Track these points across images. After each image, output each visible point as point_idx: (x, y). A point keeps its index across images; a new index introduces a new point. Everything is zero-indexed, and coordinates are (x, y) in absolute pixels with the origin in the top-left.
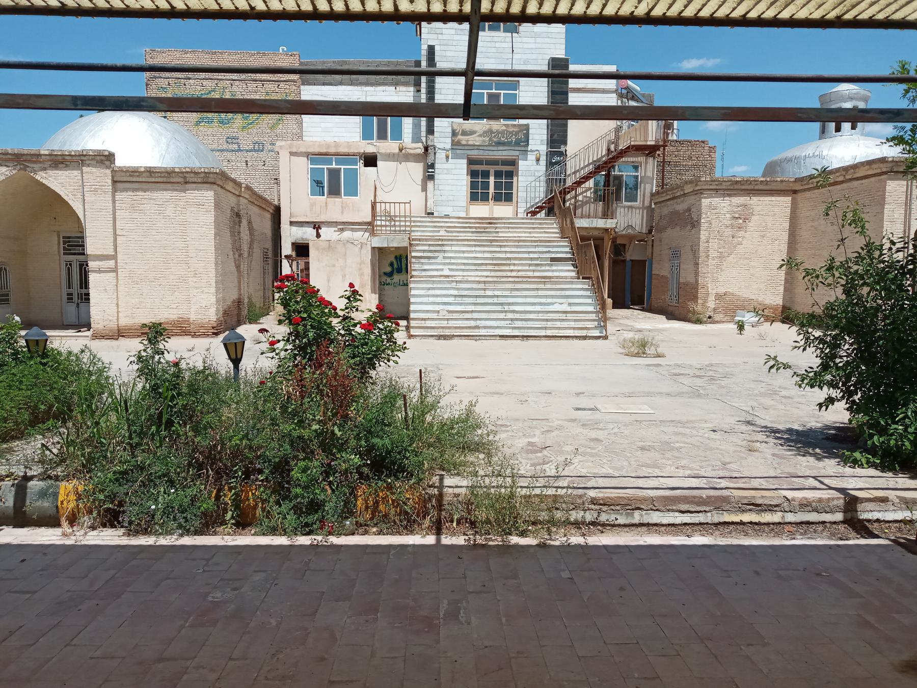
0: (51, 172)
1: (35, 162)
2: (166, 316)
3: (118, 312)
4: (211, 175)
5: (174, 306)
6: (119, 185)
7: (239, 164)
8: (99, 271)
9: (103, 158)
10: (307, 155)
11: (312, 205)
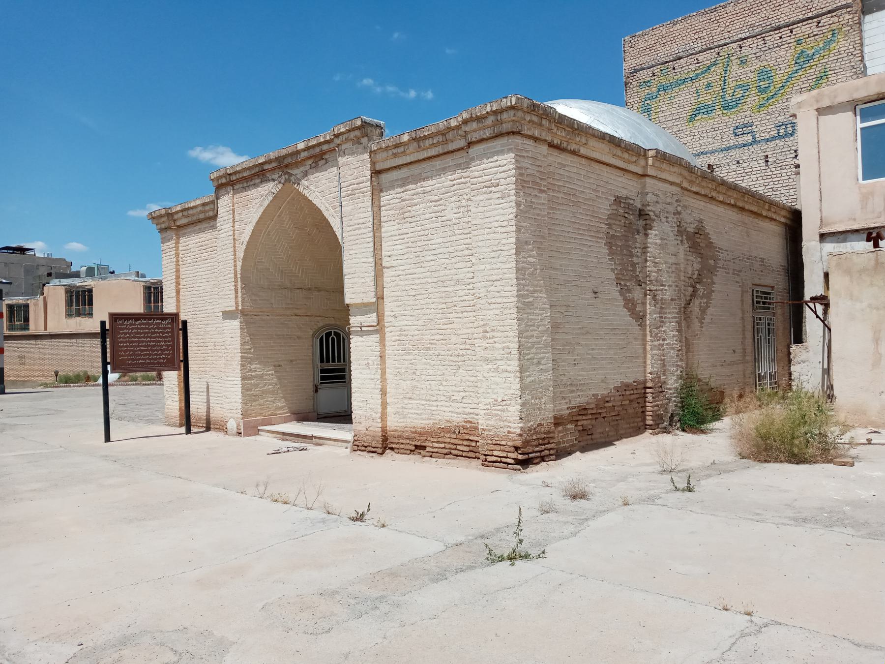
0: (311, 177)
1: (297, 164)
2: (448, 416)
3: (384, 405)
4: (505, 116)
5: (458, 397)
6: (384, 177)
7: (754, 164)
9: (357, 133)
10: (853, 106)
11: (866, 198)
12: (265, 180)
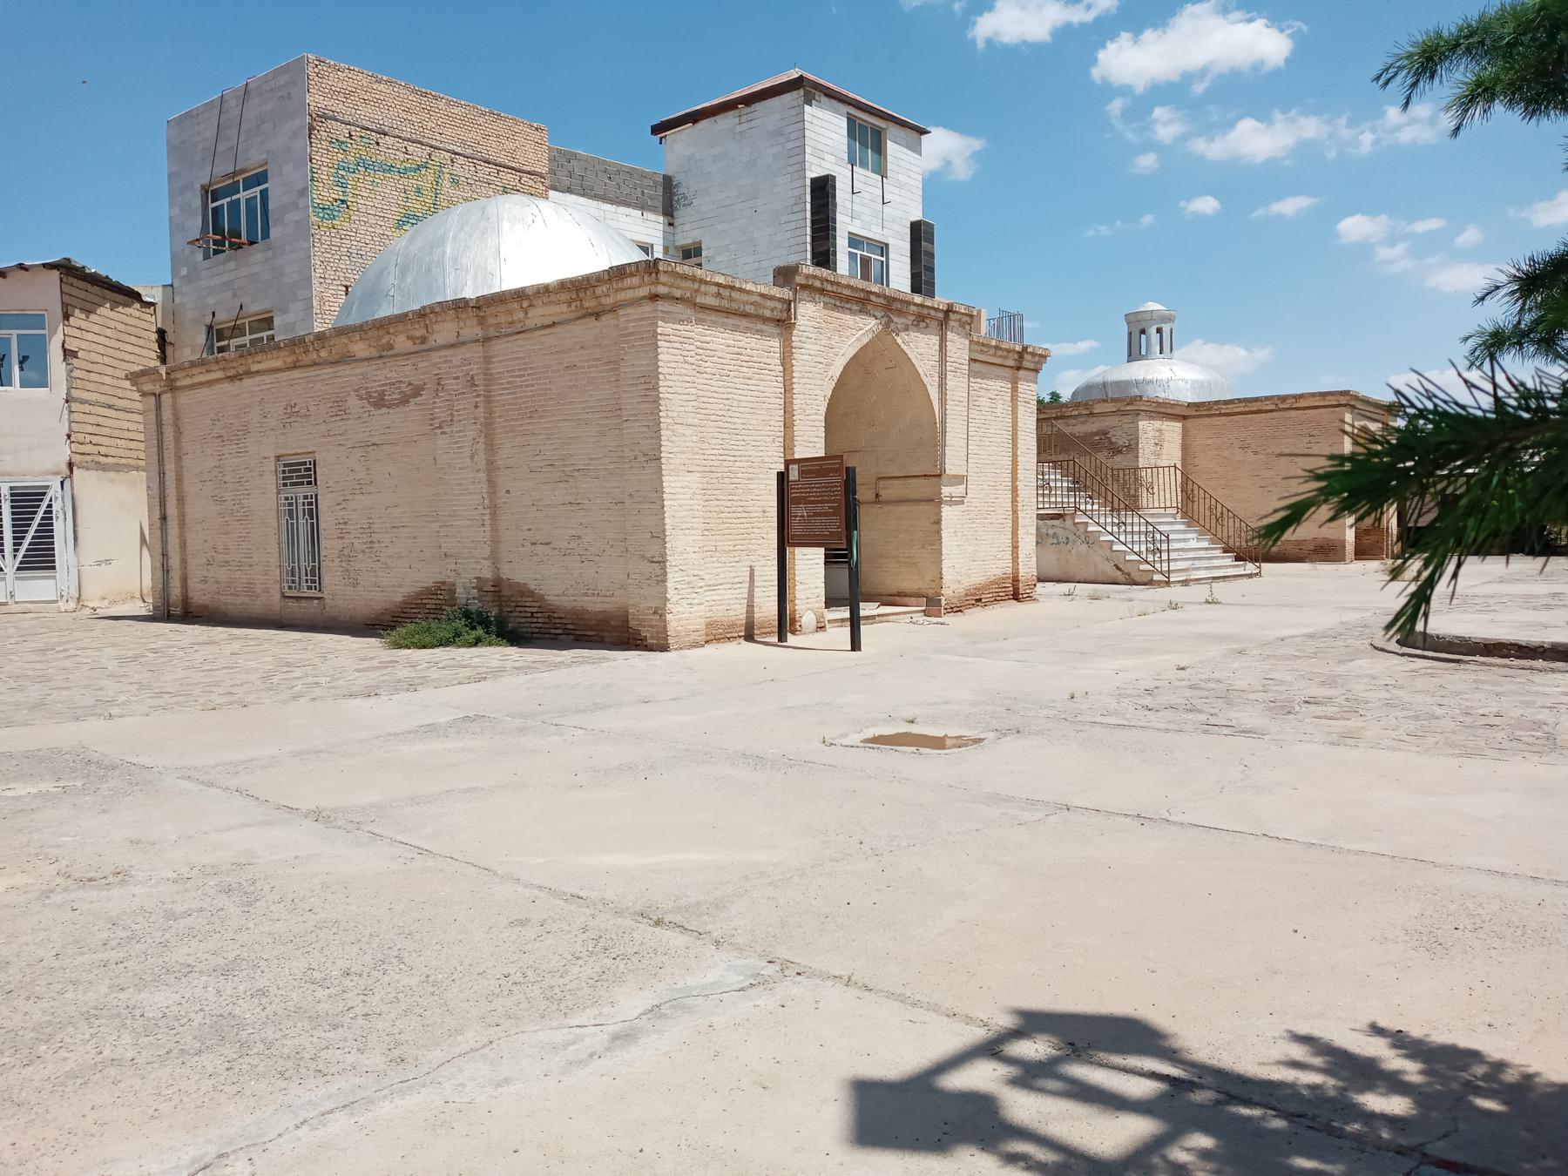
1: (900, 313)
2: (995, 571)
8: (952, 503)
12: (864, 310)
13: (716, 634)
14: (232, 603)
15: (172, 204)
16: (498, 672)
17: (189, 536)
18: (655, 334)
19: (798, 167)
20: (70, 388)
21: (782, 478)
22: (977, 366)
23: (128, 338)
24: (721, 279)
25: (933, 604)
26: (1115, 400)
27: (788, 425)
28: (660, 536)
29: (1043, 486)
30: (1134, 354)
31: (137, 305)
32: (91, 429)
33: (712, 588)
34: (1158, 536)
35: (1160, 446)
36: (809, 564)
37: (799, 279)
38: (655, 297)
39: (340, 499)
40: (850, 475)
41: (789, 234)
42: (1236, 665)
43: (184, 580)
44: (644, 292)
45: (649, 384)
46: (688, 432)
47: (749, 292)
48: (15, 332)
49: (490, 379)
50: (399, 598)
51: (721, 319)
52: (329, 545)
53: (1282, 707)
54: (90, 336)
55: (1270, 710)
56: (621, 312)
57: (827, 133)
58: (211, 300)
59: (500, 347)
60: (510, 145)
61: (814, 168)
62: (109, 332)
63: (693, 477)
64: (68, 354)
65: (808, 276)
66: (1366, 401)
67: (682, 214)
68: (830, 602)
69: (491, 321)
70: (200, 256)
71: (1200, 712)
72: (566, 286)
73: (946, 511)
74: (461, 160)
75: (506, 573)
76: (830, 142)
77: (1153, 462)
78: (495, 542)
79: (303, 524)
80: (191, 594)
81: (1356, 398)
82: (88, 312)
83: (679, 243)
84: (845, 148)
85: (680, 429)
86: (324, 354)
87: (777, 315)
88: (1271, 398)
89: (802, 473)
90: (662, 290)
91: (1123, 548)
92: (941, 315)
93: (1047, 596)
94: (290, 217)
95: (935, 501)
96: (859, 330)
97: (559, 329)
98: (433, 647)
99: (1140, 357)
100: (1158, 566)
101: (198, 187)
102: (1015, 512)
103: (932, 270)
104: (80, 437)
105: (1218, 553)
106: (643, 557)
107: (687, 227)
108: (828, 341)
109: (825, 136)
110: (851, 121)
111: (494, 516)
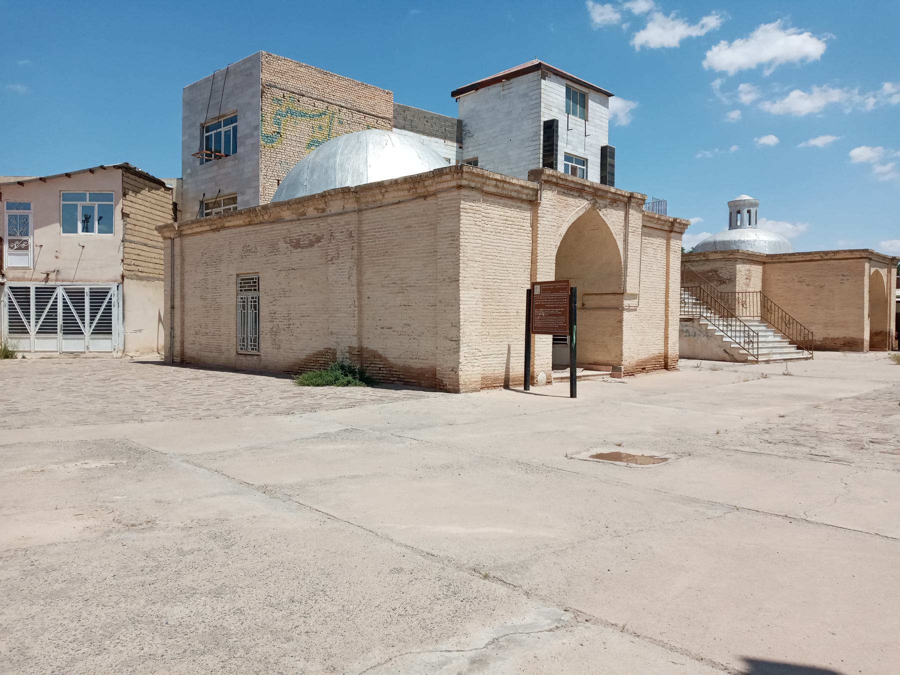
0: (609, 210)
1: (602, 197)
8: (629, 310)
12: (581, 196)
13: (487, 384)
14: (208, 356)
15: (183, 135)
16: (361, 403)
17: (186, 318)
18: (459, 209)
19: (537, 115)
20: (125, 234)
21: (530, 293)
22: (646, 230)
23: (157, 207)
24: (498, 177)
25: (616, 370)
26: (722, 252)
27: (534, 262)
28: (456, 325)
29: (682, 301)
30: (732, 225)
31: (163, 189)
32: (134, 257)
33: (485, 356)
34: (751, 333)
35: (748, 280)
36: (543, 344)
37: (544, 177)
38: (460, 187)
39: (272, 300)
40: (573, 291)
41: (529, 153)
42: (816, 415)
43: (182, 343)
44: (453, 183)
45: (454, 237)
46: (476, 265)
47: (514, 185)
48: (97, 203)
49: (361, 233)
50: (304, 357)
51: (497, 200)
52: (265, 325)
53: (856, 445)
54: (136, 206)
55: (848, 446)
56: (439, 195)
57: (554, 95)
58: (203, 187)
59: (368, 215)
60: (372, 102)
61: (546, 115)
62: (147, 204)
63: (478, 291)
64: (125, 215)
65: (549, 176)
66: (879, 255)
67: (468, 142)
68: (556, 366)
69: (363, 200)
70: (198, 163)
71: (804, 446)
72: (407, 180)
73: (626, 315)
74: (344, 110)
75: (366, 344)
76: (555, 101)
77: (744, 289)
78: (360, 326)
79: (250, 312)
80: (185, 351)
81: (872, 253)
82: (136, 192)
83: (465, 159)
84: (564, 104)
85: (471, 264)
86: (266, 217)
87: (530, 198)
88: (819, 253)
89: (542, 290)
90: (464, 182)
91: (729, 340)
92: (626, 199)
93: (685, 367)
94: (248, 141)
95: (620, 309)
96: (578, 207)
97: (402, 205)
98: (323, 385)
99: (736, 227)
100: (751, 351)
101: (198, 124)
102: (667, 316)
103: (613, 174)
104: (128, 261)
105: (786, 344)
106: (446, 337)
107: (470, 149)
108: (559, 213)
109: (553, 97)
110: (568, 89)
111: (360, 312)
